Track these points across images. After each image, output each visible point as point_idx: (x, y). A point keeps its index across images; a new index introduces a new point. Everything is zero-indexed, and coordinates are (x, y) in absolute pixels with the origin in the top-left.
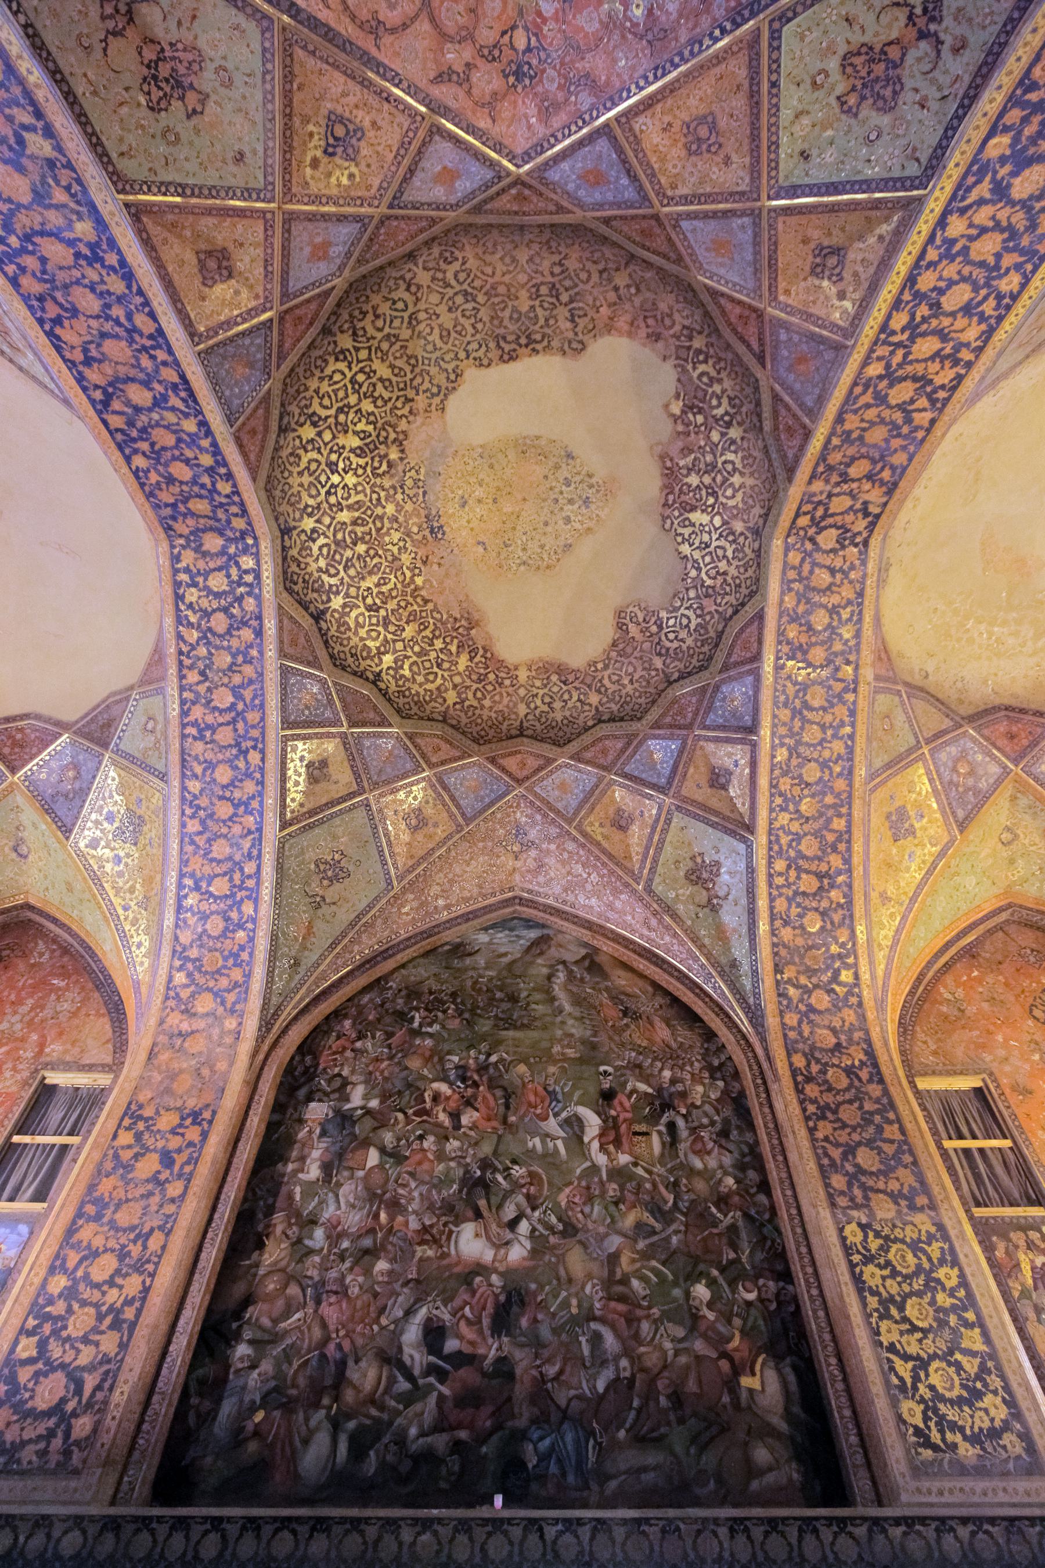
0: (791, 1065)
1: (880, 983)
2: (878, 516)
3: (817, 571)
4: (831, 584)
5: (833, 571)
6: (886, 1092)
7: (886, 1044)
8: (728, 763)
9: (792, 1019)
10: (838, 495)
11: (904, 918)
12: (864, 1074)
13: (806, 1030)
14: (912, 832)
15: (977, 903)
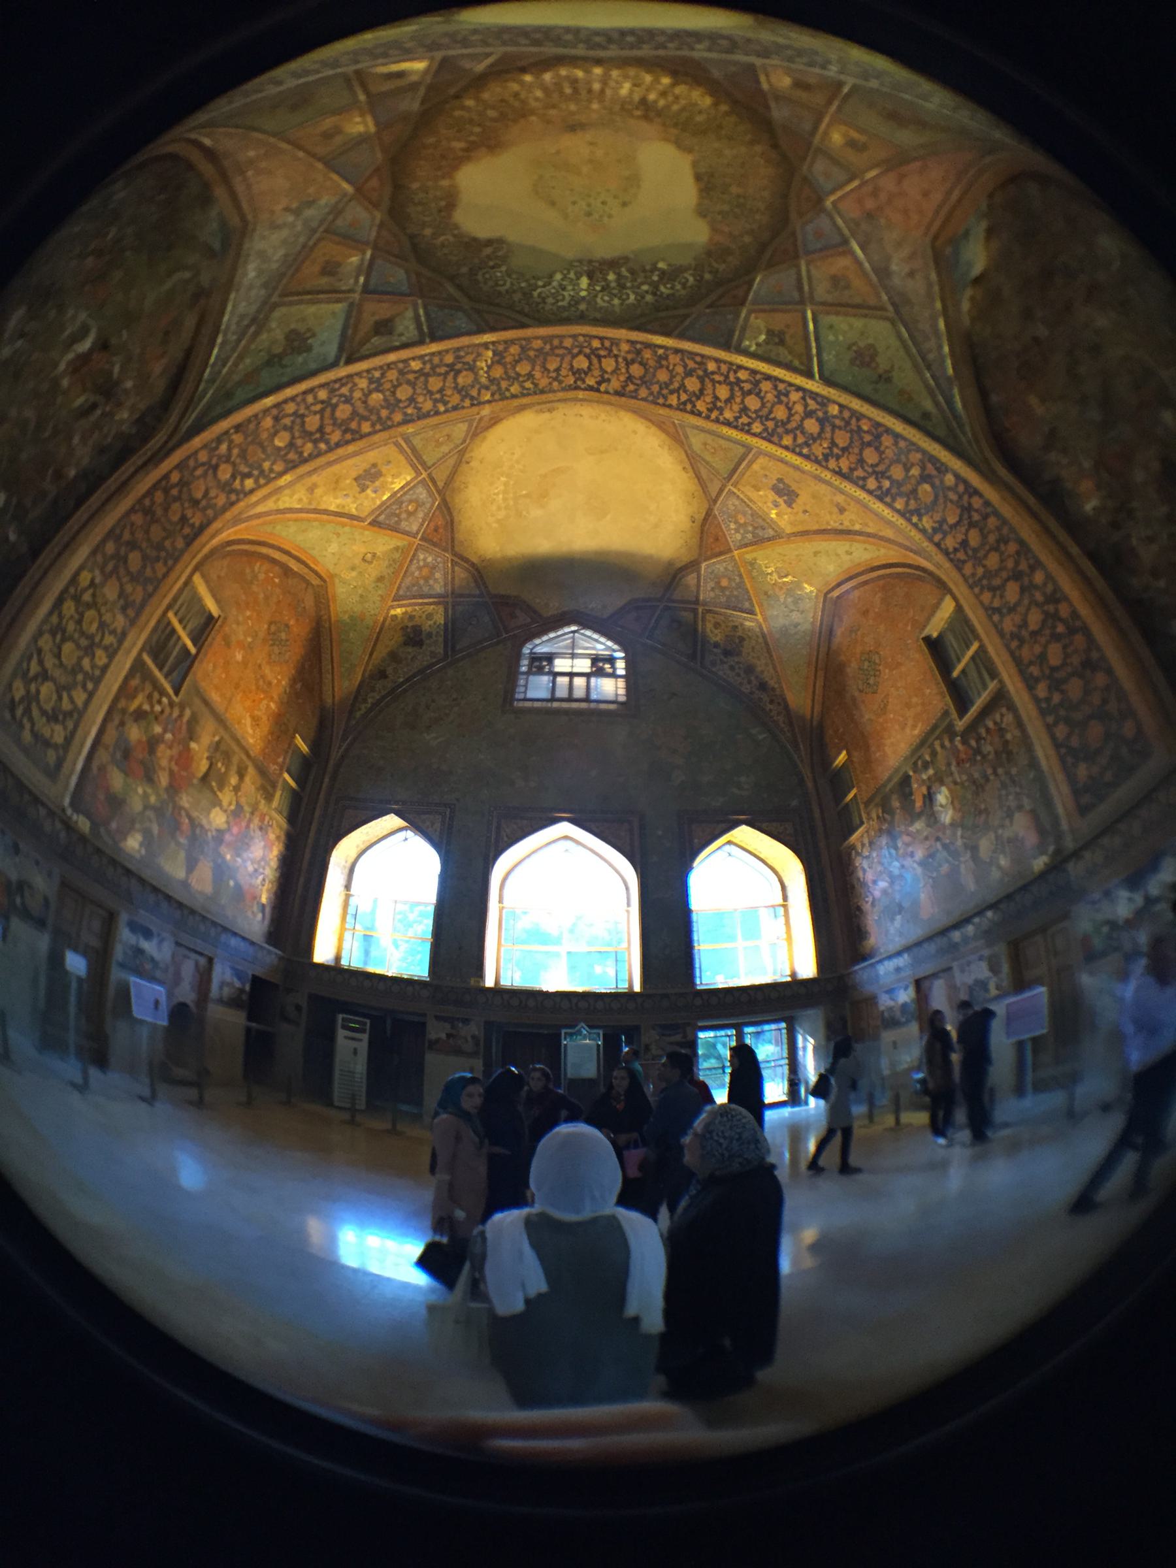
0: (171, 472)
1: (252, 512)
2: (598, 390)
3: (558, 359)
4: (549, 371)
5: (557, 370)
6: (182, 552)
7: (213, 536)
8: (400, 329)
9: (203, 457)
10: (617, 362)
11: (301, 511)
12: (187, 530)
13: (199, 472)
14: (363, 489)
15: (319, 559)
